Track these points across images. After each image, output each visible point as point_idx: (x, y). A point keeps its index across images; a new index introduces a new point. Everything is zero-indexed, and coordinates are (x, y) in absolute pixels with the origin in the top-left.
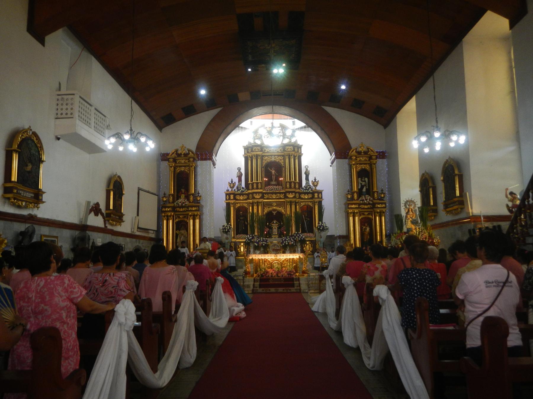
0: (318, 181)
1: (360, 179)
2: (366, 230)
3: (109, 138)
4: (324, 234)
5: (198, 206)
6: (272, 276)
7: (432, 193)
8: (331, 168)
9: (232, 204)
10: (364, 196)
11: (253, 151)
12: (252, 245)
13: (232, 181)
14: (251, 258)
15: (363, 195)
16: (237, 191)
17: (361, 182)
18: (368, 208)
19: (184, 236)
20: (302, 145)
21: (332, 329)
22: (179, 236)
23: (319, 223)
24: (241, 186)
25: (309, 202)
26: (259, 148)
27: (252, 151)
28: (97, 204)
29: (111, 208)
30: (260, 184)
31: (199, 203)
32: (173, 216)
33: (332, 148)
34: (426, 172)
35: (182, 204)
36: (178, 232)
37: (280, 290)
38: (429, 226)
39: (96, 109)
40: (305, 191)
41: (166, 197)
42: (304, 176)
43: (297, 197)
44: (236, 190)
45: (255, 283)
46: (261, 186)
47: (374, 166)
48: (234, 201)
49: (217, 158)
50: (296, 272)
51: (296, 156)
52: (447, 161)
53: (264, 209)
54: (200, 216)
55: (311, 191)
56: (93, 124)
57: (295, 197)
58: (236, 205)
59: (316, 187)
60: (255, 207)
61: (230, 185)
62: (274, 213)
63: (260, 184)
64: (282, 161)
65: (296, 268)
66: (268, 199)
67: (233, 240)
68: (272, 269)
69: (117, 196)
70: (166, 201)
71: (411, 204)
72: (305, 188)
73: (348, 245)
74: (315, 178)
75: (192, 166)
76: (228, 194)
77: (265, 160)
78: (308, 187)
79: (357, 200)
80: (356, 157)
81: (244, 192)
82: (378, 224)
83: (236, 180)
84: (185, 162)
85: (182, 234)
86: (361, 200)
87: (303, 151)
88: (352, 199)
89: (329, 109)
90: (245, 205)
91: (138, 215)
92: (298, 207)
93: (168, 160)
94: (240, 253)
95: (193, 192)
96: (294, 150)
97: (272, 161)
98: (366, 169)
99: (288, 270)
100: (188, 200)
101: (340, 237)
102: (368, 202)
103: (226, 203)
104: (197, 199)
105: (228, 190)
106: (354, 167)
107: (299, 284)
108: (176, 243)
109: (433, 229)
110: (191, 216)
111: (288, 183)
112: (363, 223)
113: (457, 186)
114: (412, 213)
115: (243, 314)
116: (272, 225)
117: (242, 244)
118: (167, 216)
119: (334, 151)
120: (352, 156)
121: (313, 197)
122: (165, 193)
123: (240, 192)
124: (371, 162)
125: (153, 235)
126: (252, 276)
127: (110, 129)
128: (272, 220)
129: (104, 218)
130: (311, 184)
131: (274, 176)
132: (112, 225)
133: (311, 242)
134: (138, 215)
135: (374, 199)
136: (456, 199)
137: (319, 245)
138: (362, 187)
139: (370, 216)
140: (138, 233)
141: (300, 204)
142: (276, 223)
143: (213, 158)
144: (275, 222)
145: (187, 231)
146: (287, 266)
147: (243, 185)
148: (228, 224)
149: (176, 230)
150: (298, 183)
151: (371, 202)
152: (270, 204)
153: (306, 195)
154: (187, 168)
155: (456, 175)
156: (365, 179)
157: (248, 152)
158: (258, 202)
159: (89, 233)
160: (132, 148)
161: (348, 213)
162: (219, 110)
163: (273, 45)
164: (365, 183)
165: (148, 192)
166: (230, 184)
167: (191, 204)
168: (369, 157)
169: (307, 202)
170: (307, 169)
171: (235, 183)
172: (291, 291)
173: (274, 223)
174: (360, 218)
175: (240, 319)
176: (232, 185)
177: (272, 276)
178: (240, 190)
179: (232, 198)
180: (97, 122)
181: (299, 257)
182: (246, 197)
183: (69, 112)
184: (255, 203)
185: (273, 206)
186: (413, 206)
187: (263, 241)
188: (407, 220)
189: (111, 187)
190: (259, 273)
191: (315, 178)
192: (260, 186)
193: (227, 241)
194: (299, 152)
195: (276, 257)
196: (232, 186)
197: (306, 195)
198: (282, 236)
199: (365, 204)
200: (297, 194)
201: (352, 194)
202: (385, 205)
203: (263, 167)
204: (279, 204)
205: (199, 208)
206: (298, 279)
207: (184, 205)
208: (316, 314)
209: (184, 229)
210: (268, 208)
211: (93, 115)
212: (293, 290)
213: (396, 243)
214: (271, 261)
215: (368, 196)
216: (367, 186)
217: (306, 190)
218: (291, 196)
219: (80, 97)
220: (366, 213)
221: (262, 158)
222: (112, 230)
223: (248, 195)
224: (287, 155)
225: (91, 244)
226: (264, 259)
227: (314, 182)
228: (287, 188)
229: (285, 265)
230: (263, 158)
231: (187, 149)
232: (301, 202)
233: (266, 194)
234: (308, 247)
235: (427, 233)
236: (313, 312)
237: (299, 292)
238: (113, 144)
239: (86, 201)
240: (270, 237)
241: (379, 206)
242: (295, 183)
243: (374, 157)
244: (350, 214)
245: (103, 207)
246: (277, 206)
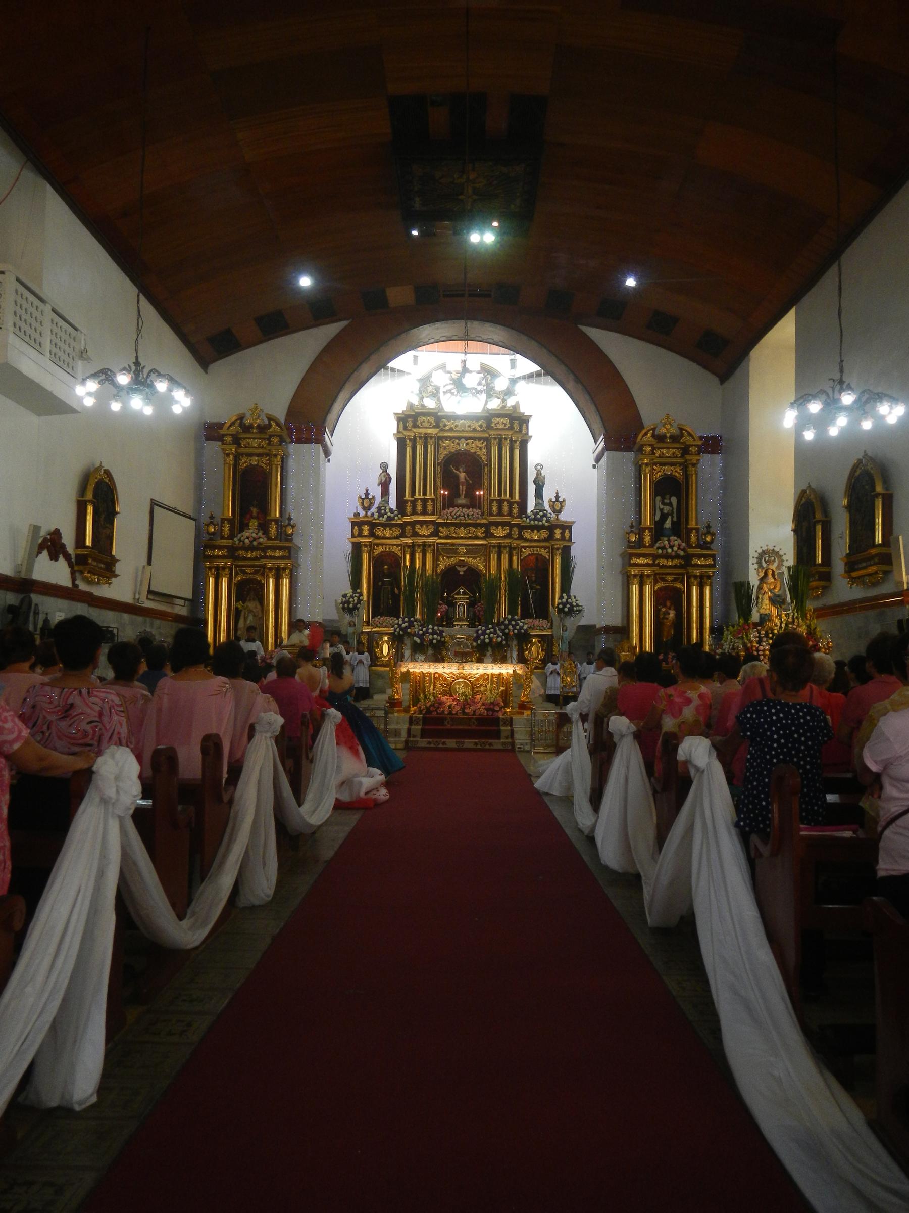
0: (564, 501)
1: (658, 498)
2: (667, 616)
3: (83, 381)
4: (572, 623)
6: (450, 713)
7: (820, 536)
8: (595, 470)
9: (366, 546)
10: (666, 539)
11: (418, 427)
12: (407, 642)
13: (367, 494)
14: (404, 669)
15: (664, 536)
16: (379, 517)
17: (662, 507)
18: (675, 566)
19: (254, 616)
20: (531, 416)
21: (580, 831)
22: (243, 614)
23: (561, 598)
24: (387, 505)
25: (541, 548)
26: (432, 419)
27: (415, 426)
28: (57, 533)
29: (89, 543)
30: (430, 503)
31: (291, 541)
32: (231, 569)
33: (598, 425)
34: (809, 486)
35: (251, 542)
36: (240, 605)
37: (469, 743)
38: (810, 610)
39: (54, 310)
40: (532, 522)
41: (215, 525)
42: (531, 489)
43: (515, 537)
44: (376, 515)
45: (413, 727)
46: (434, 507)
47: (692, 470)
48: (371, 539)
49: (334, 439)
50: (506, 705)
51: (515, 441)
52: (860, 461)
53: (438, 560)
54: (291, 570)
55: (547, 524)
56: (47, 346)
57: (509, 536)
58: (374, 549)
59: (557, 515)
60: (418, 556)
61: (362, 503)
62: (462, 570)
63: (430, 503)
64: (484, 450)
65: (505, 696)
66: (447, 537)
67: (366, 629)
68: (451, 696)
69: (103, 516)
70: (213, 534)
71: (773, 558)
72: (533, 516)
73: (626, 647)
74: (557, 494)
75: (276, 456)
76: (357, 524)
77: (445, 448)
78: (541, 513)
79: (651, 546)
80: (653, 449)
81: (393, 519)
82: (695, 604)
83: (376, 492)
84: (260, 444)
85: (250, 611)
86: (658, 548)
87: (533, 428)
88: (640, 543)
89: (595, 334)
90: (396, 550)
91: (149, 562)
92: (515, 558)
93: (220, 438)
94: (381, 658)
95: (278, 515)
96: (511, 428)
97: (460, 450)
98: (674, 475)
99: (486, 699)
100: (266, 532)
101: (608, 630)
102: (676, 552)
103: (353, 543)
104: (285, 531)
105: (357, 515)
106: (647, 471)
107: (512, 732)
108: (236, 630)
109: (817, 617)
110: (270, 569)
111: (495, 504)
112: (659, 599)
113: (879, 520)
114: (773, 580)
115: (383, 794)
116: (456, 599)
117: (386, 638)
118: (217, 568)
119: (604, 431)
120: (643, 446)
121: (551, 537)
122: (212, 514)
123: (384, 519)
124: (686, 461)
125: (182, 610)
126: (407, 710)
127: (88, 359)
128: (457, 586)
129: (71, 565)
130: (547, 506)
131: (462, 485)
132: (90, 582)
133: (542, 638)
134: (149, 562)
135: (689, 545)
136: (873, 551)
137: (559, 648)
138: (664, 517)
139: (679, 585)
140: (148, 604)
141: (522, 551)
142: (464, 593)
143: (324, 438)
144: (462, 591)
145: (262, 604)
146: (486, 691)
147: (393, 503)
148: (354, 592)
149: (237, 601)
150: (517, 503)
151: (682, 553)
152: (451, 551)
153: (536, 531)
154: (265, 459)
155: (877, 495)
156: (670, 499)
157: (405, 428)
158: (424, 545)
159: (35, 598)
160: (138, 404)
161: (628, 577)
162: (343, 324)
163: (472, 176)
164: (671, 509)
165: (174, 511)
166: (363, 500)
167: (271, 543)
168: (681, 448)
169: (537, 547)
170: (539, 473)
171: (374, 498)
172: (492, 747)
173: (459, 593)
174: (656, 588)
175: (377, 804)
176: (366, 500)
177: (450, 713)
178: (386, 516)
179: (366, 533)
180: (58, 341)
181: (514, 671)
182: (397, 531)
184: (419, 546)
185: (459, 554)
186: (776, 564)
187: (434, 633)
188: (760, 596)
189: (89, 495)
190: (421, 704)
191: (557, 494)
192: (430, 508)
193: (351, 630)
194: (524, 431)
195: (460, 671)
196: (366, 506)
197: (536, 531)
198: (477, 623)
199: (668, 557)
200: (515, 529)
201: (641, 532)
202: (714, 560)
203: (439, 464)
204: (473, 551)
205: (290, 552)
206: (510, 722)
207: (255, 543)
208: (546, 799)
209: (254, 600)
210: (448, 558)
211: (47, 325)
212: (497, 744)
213: (733, 646)
214: (450, 680)
215: (676, 538)
216: (675, 515)
217: (534, 520)
218: (500, 532)
219: (18, 280)
220: (670, 578)
221: (438, 443)
222: (90, 595)
223: (403, 526)
224: (495, 439)
225: (40, 624)
226: (435, 674)
227: (554, 503)
228: (491, 514)
229: (482, 689)
230: (440, 442)
231: (266, 414)
232: (522, 547)
233: (443, 528)
234: (535, 650)
235: (804, 627)
236: (538, 795)
237: (511, 749)
238: (97, 395)
239: (31, 525)
240: (450, 624)
241: (699, 562)
242: (511, 504)
243: (694, 450)
244: (632, 577)
245: (68, 539)
246: (469, 553)
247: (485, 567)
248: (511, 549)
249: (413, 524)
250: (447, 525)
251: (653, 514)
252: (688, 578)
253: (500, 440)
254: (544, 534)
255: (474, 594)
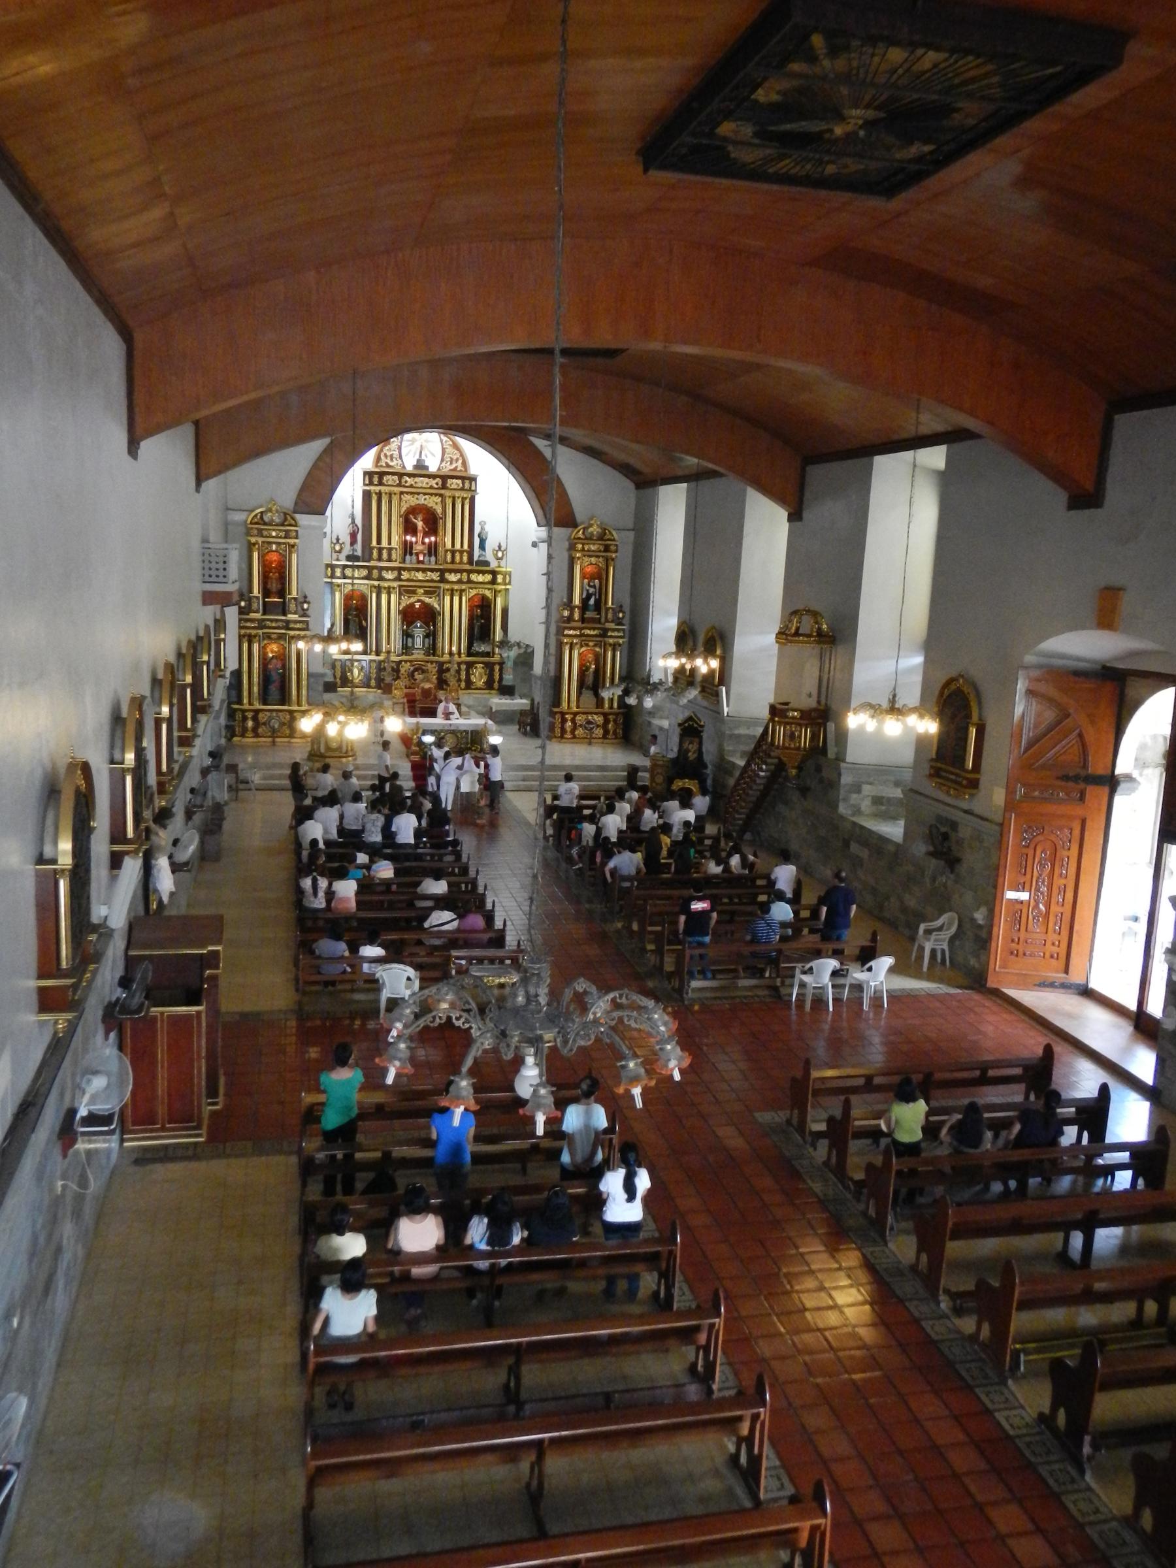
5: (307, 622)
13: (338, 540)
27: (381, 483)
51: (466, 498)
57: (460, 582)
60: (384, 597)
62: (417, 605)
70: (244, 608)
80: (583, 544)
83: (346, 539)
87: (481, 486)
90: (365, 590)
121: (494, 582)
138: (589, 596)
142: (421, 627)
158: (389, 588)
173: (416, 627)
182: (364, 573)
183: (221, 573)
184: (385, 588)
192: (394, 556)
194: (473, 488)
218: (452, 577)
220: (591, 644)
246: (426, 593)
247: (439, 605)
248: (462, 591)
249: (381, 569)
250: (409, 570)
251: (581, 594)
252: (605, 645)
253: (454, 498)
254: (489, 577)
255: (429, 627)
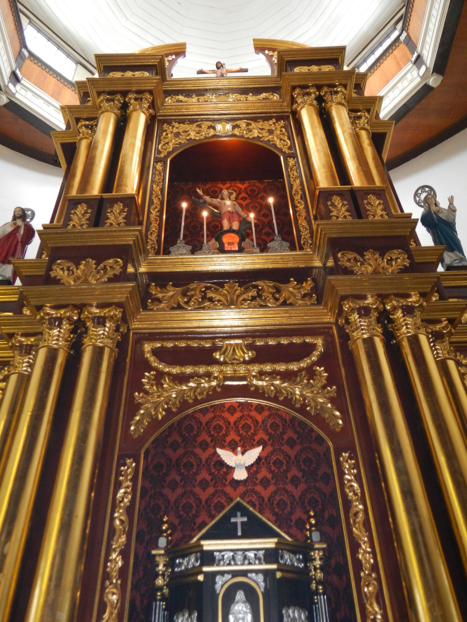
77: (177, 135)
144: (239, 520)
